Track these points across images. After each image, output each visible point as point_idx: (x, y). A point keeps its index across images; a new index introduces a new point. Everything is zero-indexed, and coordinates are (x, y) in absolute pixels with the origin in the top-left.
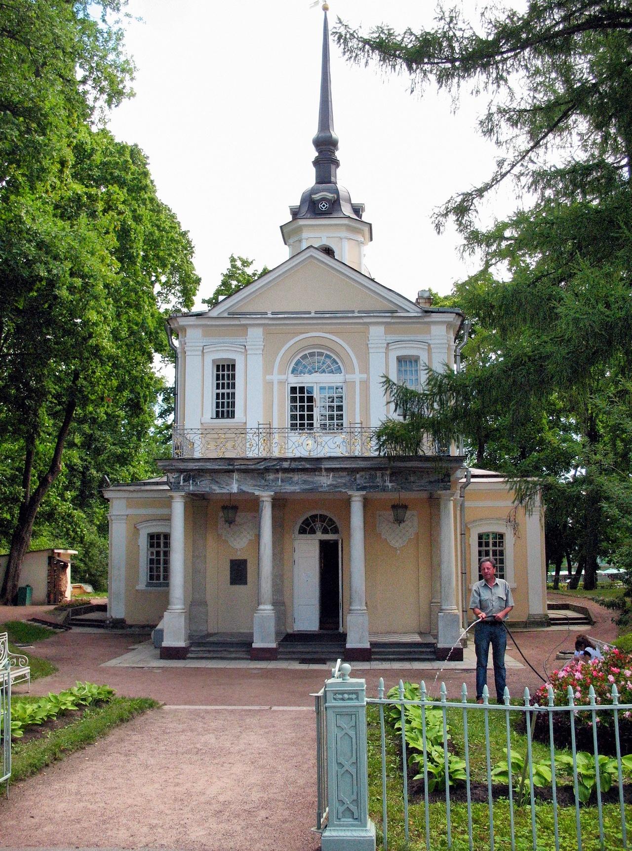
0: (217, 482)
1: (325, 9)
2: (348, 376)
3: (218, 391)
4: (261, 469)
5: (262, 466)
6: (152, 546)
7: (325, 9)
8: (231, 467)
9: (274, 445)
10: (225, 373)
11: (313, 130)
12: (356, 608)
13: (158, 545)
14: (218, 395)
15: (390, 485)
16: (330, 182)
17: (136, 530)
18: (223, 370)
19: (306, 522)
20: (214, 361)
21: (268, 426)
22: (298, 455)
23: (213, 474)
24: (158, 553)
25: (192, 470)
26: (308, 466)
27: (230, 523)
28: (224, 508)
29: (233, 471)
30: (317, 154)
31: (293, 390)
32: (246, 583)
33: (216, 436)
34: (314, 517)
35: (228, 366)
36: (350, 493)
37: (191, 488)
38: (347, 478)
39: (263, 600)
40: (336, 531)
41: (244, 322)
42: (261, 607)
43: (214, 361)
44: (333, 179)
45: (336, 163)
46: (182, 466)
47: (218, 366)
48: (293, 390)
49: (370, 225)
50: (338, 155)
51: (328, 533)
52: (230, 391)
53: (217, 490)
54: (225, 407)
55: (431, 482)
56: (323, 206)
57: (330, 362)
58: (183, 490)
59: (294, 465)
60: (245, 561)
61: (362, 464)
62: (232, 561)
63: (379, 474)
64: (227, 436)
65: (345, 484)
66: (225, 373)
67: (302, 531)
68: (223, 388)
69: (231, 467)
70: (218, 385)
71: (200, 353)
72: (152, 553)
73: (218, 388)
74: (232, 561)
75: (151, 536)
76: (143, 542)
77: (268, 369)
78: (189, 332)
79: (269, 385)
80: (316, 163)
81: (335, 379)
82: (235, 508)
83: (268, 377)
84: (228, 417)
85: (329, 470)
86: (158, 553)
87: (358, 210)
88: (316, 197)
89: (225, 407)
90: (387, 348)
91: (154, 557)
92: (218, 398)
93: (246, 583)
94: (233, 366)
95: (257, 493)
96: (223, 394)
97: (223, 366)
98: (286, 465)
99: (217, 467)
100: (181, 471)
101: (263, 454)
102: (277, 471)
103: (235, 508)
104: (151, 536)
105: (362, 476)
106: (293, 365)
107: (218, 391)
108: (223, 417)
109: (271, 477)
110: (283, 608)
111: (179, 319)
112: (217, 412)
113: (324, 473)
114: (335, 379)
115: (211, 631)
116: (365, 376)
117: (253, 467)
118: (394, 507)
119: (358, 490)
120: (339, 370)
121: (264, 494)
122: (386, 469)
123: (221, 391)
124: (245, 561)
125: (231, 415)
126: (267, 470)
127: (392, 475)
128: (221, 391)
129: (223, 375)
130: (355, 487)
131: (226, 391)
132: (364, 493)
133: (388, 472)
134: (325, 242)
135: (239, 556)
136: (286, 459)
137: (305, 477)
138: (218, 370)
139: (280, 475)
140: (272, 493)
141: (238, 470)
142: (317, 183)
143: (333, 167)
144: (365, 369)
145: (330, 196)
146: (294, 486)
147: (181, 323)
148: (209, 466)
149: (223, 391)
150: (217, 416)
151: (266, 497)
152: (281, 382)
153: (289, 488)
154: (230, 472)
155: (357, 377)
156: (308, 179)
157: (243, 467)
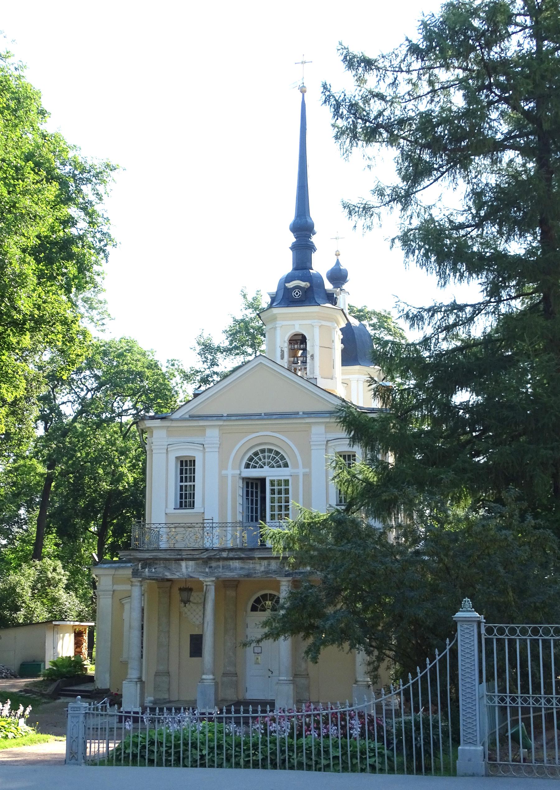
0: (169, 569)
1: (303, 91)
3: (182, 484)
5: (205, 555)
7: (303, 91)
9: (215, 538)
10: (186, 467)
11: (290, 216)
14: (181, 486)
18: (186, 465)
19: (257, 601)
20: (177, 458)
21: (211, 521)
25: (148, 559)
26: (243, 556)
27: (185, 603)
28: (180, 589)
29: (182, 560)
30: (295, 240)
33: (168, 530)
34: (264, 597)
35: (190, 461)
36: (278, 579)
41: (202, 423)
43: (177, 458)
46: (139, 555)
50: (314, 239)
53: (168, 575)
54: (186, 499)
56: (297, 294)
59: (231, 555)
62: (191, 636)
64: (178, 529)
66: (186, 467)
67: (254, 609)
68: (186, 481)
70: (182, 478)
71: (165, 451)
73: (181, 481)
77: (223, 465)
78: (156, 433)
79: (223, 479)
80: (294, 248)
82: (191, 590)
83: (224, 472)
88: (290, 285)
89: (186, 499)
92: (181, 490)
94: (194, 461)
96: (186, 486)
97: (186, 461)
98: (225, 554)
99: (168, 557)
100: (140, 560)
102: (219, 559)
103: (191, 590)
106: (245, 460)
107: (182, 484)
109: (214, 564)
110: (234, 678)
111: (146, 422)
112: (181, 502)
113: (257, 561)
115: (172, 699)
117: (197, 556)
119: (287, 576)
120: (286, 465)
123: (184, 484)
125: (192, 505)
126: (210, 559)
128: (184, 484)
129: (186, 469)
131: (188, 484)
132: (290, 578)
134: (298, 328)
135: (196, 632)
136: (224, 550)
138: (182, 465)
139: (221, 563)
140: (214, 579)
142: (295, 269)
144: (307, 463)
145: (303, 284)
147: (148, 426)
149: (186, 484)
150: (181, 506)
152: (233, 476)
153: (229, 575)
156: (286, 265)
157: (189, 556)
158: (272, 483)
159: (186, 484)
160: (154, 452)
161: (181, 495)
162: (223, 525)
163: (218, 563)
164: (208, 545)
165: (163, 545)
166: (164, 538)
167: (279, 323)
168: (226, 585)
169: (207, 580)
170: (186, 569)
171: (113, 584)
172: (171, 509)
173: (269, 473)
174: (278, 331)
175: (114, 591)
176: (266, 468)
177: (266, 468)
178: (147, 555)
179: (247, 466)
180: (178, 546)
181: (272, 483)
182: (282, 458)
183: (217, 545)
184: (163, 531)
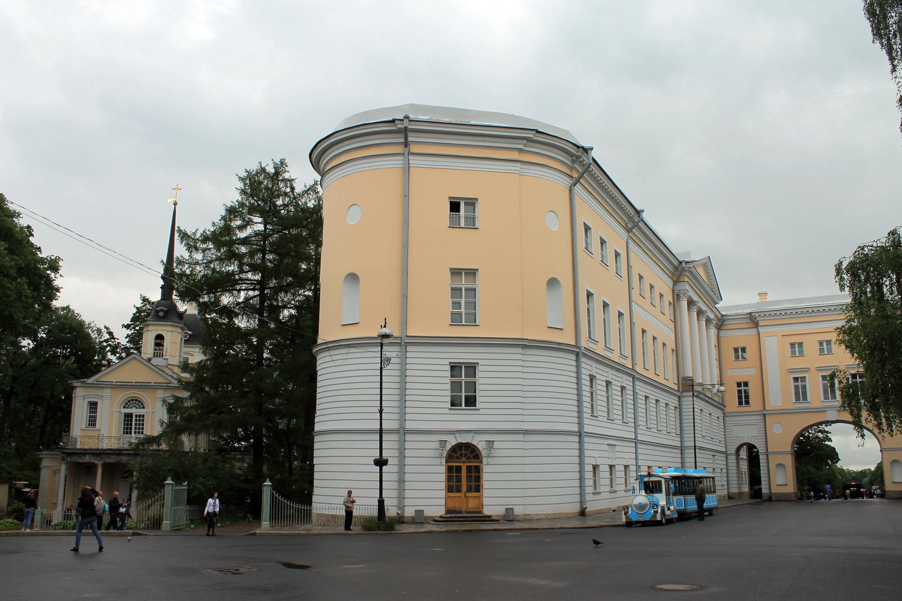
1: (175, 204)
4: (99, 453)
7: (175, 204)
10: (93, 406)
53: (80, 461)
54: (92, 422)
56: (161, 314)
57: (139, 403)
66: (93, 406)
78: (78, 389)
81: (140, 411)
89: (92, 422)
114: (140, 411)
125: (94, 425)
134: (160, 332)
146: (112, 460)
151: (99, 463)
154: (85, 454)
158: (136, 416)
162: (109, 437)
164: (100, 447)
165: (78, 446)
166: (79, 443)
168: (107, 468)
170: (87, 459)
172: (83, 427)
173: (135, 411)
180: (86, 447)
183: (105, 447)
184: (79, 439)
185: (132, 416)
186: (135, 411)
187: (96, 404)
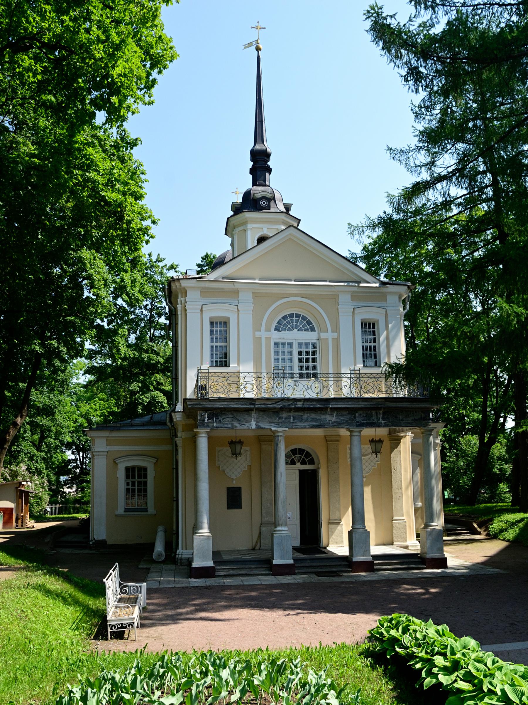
0: (238, 420)
2: (322, 334)
3: (212, 344)
5: (279, 406)
6: (127, 477)
7: (258, 49)
8: (252, 406)
10: (220, 327)
12: (358, 526)
13: (134, 477)
14: (212, 347)
15: (383, 422)
16: (266, 185)
17: (115, 463)
22: (308, 396)
23: (235, 413)
24: (133, 484)
26: (318, 406)
29: (252, 410)
30: (252, 163)
31: (276, 344)
32: (240, 507)
37: (215, 424)
38: (348, 417)
39: (280, 523)
40: (312, 462)
42: (279, 528)
43: (210, 318)
44: (267, 183)
45: (269, 170)
47: (212, 323)
48: (276, 344)
49: (300, 220)
51: (306, 464)
52: (223, 344)
55: (415, 420)
58: (208, 426)
59: (306, 405)
60: (240, 489)
61: (362, 405)
62: (229, 489)
63: (374, 412)
64: (246, 379)
65: (347, 421)
66: (220, 327)
68: (217, 342)
69: (252, 406)
72: (128, 484)
73: (212, 342)
74: (229, 489)
75: (127, 469)
76: (121, 474)
80: (252, 171)
81: (310, 337)
83: (258, 334)
84: (221, 366)
85: (334, 409)
86: (133, 484)
87: (288, 208)
90: (353, 312)
91: (130, 487)
93: (240, 507)
95: (273, 429)
96: (217, 347)
98: (299, 405)
99: (240, 406)
100: (206, 410)
101: (279, 395)
102: (290, 410)
103: (241, 443)
104: (127, 469)
105: (360, 415)
106: (275, 324)
108: (217, 366)
109: (284, 415)
114: (310, 337)
116: (336, 334)
118: (372, 441)
120: (313, 329)
121: (280, 430)
122: (380, 409)
123: (215, 344)
124: (240, 489)
126: (282, 409)
127: (384, 414)
130: (355, 424)
131: (219, 344)
133: (381, 412)
135: (234, 484)
136: (299, 400)
137: (313, 415)
141: (257, 409)
143: (267, 174)
148: (233, 405)
149: (217, 344)
155: (329, 335)
157: (263, 406)
158: (300, 345)
159: (217, 344)
160: (188, 311)
161: (212, 354)
163: (289, 414)
167: (249, 226)
169: (279, 430)
171: (108, 444)
174: (249, 233)
175: (107, 452)
176: (295, 330)
177: (295, 330)
178: (218, 405)
179: (277, 329)
181: (300, 345)
182: (309, 323)
185: (291, 345)
186: (297, 336)
187: (225, 323)
